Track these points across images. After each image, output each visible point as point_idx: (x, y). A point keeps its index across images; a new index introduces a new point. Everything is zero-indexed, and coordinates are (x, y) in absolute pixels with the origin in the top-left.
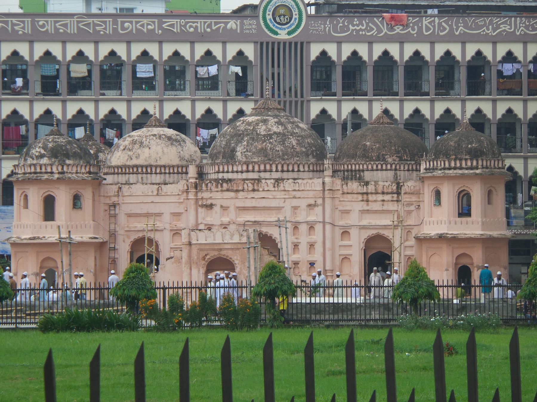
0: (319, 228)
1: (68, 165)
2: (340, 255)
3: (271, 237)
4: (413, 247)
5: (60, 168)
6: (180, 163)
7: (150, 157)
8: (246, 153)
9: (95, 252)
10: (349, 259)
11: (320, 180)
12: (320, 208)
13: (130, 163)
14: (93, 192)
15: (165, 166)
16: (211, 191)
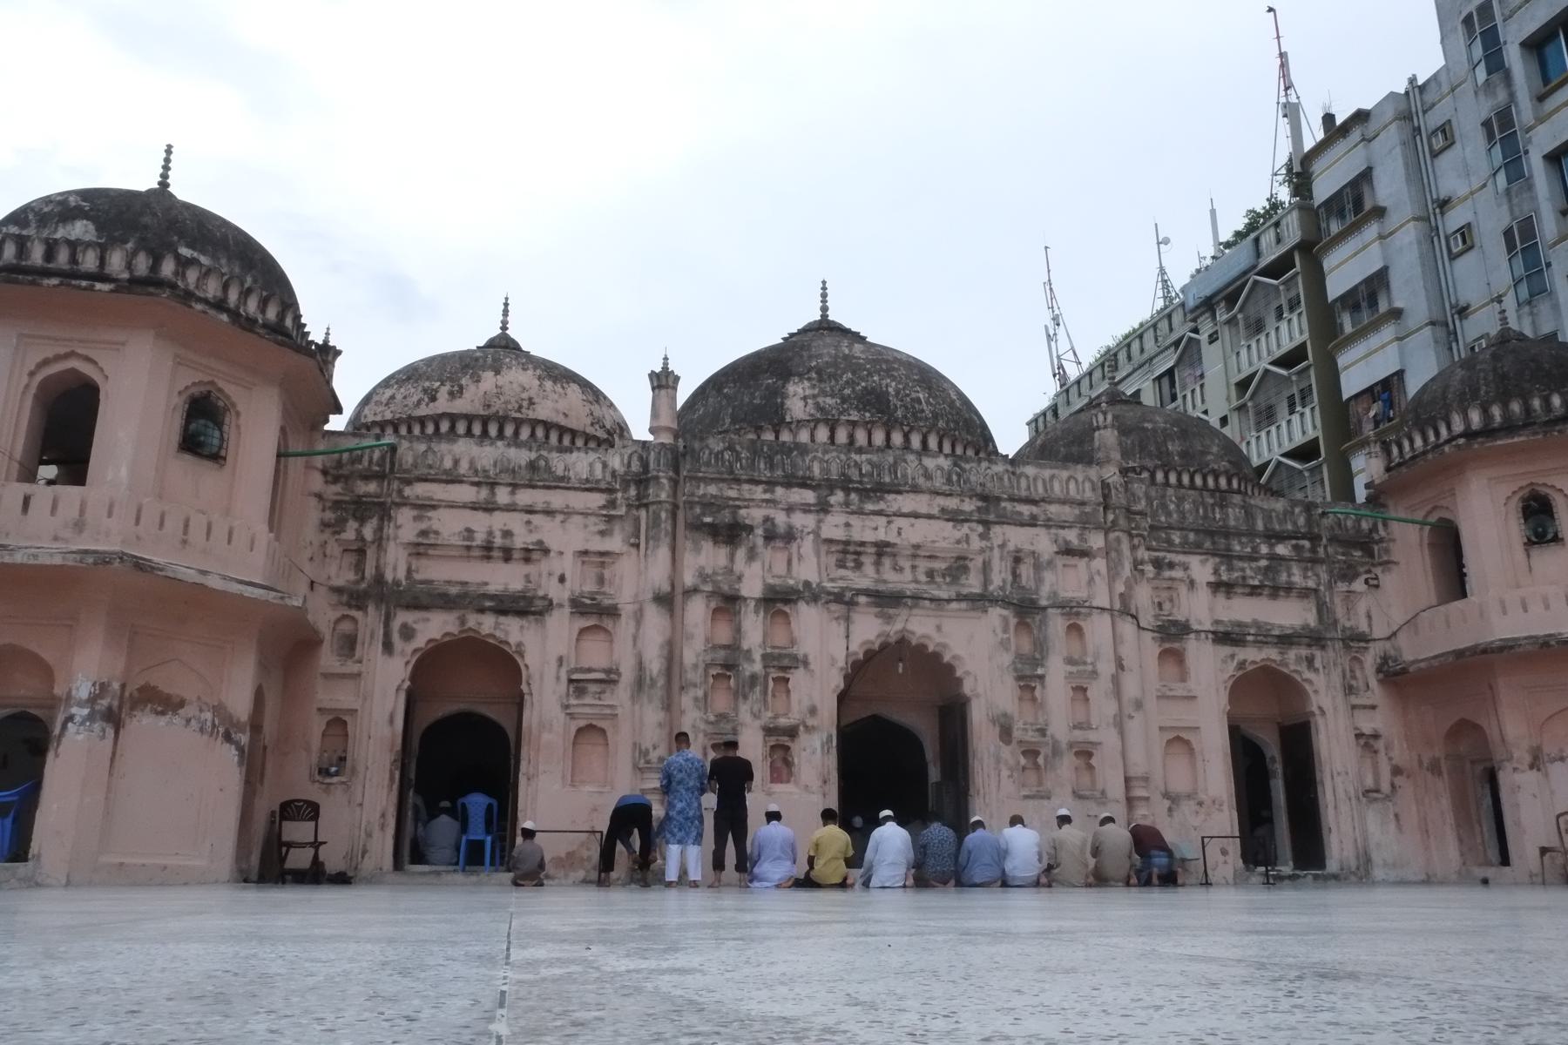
0: (1098, 629)
1: (184, 264)
2: (1161, 728)
3: (937, 656)
4: (1373, 707)
5: (142, 264)
6: (590, 430)
7: (498, 395)
8: (820, 400)
9: (263, 666)
10: (1187, 743)
11: (1093, 472)
12: (1099, 564)
13: (423, 411)
14: (283, 430)
15: (548, 426)
16: (738, 481)
